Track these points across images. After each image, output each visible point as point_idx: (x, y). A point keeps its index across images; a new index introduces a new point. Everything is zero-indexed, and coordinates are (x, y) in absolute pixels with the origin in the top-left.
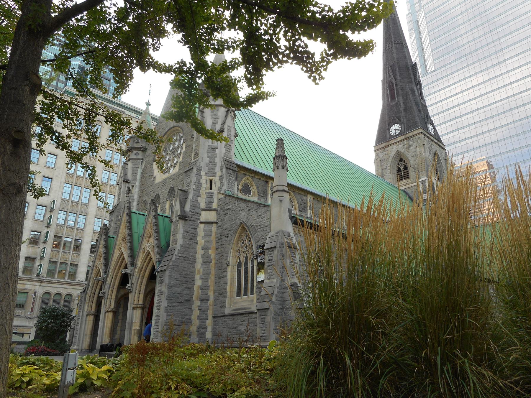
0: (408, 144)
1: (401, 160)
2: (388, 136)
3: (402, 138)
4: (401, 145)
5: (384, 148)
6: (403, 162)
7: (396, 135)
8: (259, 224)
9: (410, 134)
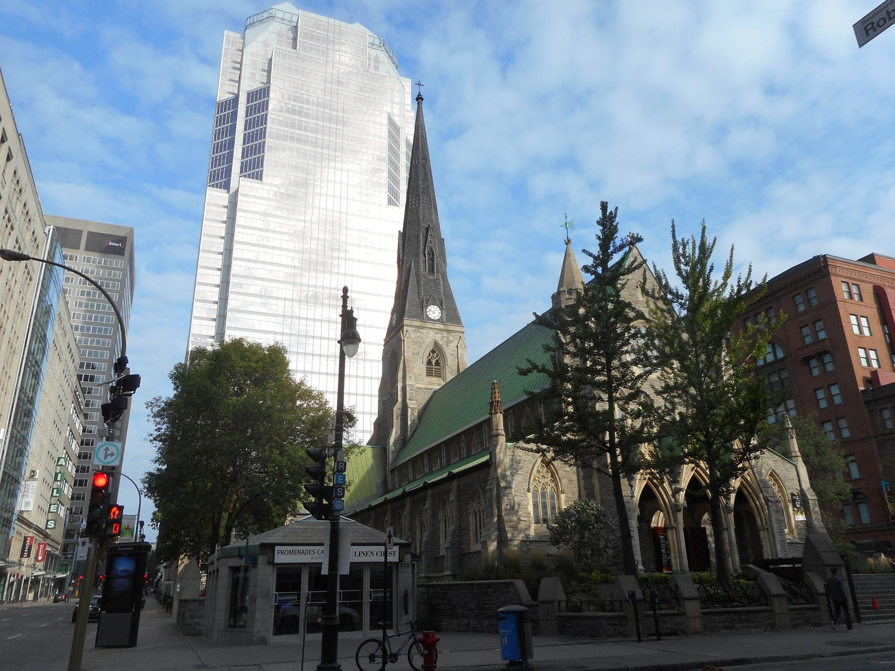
0: (448, 338)
1: (433, 351)
2: (425, 315)
3: (442, 327)
4: (440, 336)
5: (419, 327)
6: (435, 355)
7: (434, 320)
8: (788, 475)
9: (451, 328)
